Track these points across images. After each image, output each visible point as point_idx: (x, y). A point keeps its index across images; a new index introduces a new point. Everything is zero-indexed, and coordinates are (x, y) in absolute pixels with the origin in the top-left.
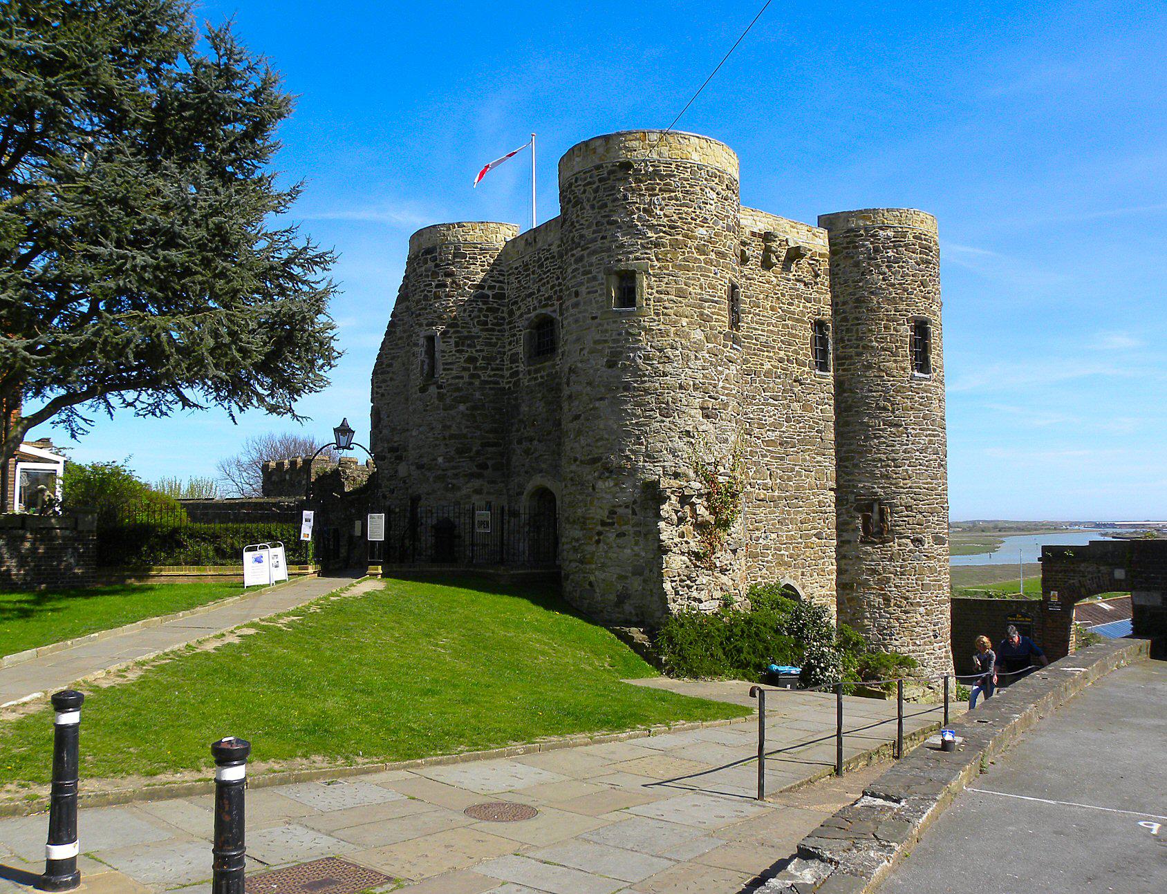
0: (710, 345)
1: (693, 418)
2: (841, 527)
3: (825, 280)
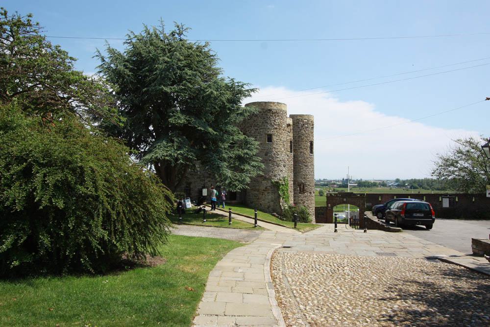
1: (282, 168)
2: (294, 190)
3: (292, 131)
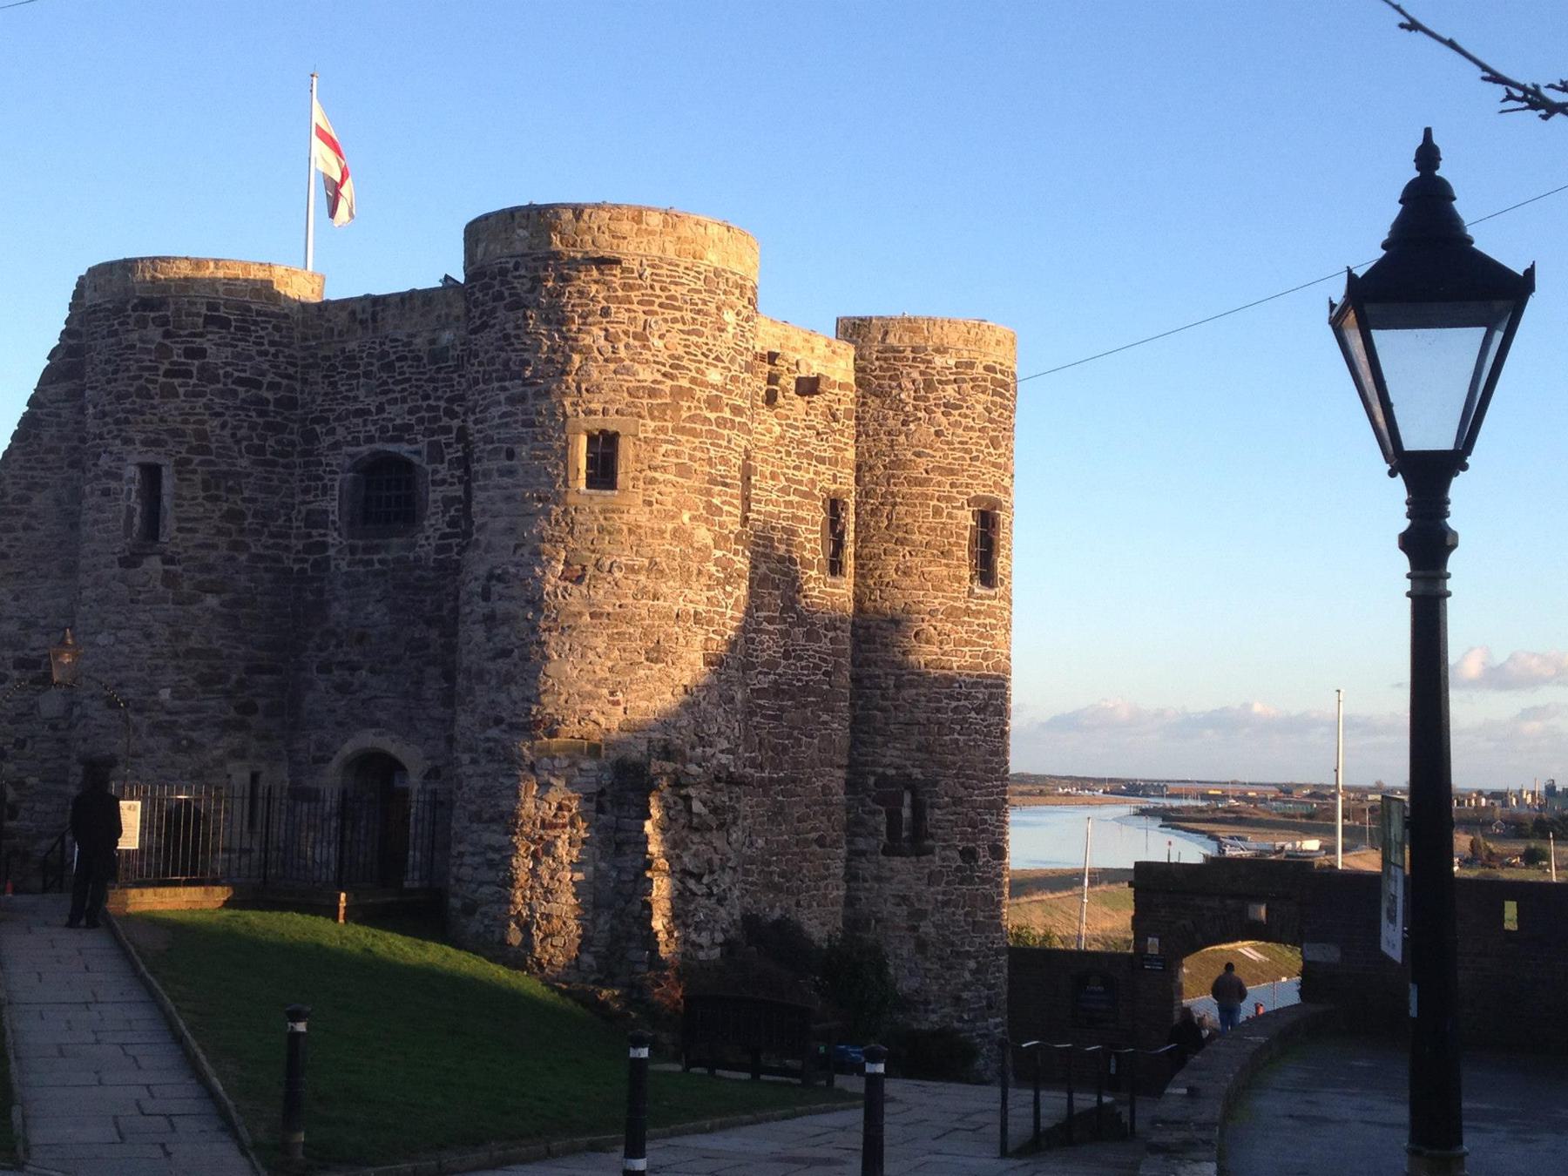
0: (719, 553)
2: (854, 827)
